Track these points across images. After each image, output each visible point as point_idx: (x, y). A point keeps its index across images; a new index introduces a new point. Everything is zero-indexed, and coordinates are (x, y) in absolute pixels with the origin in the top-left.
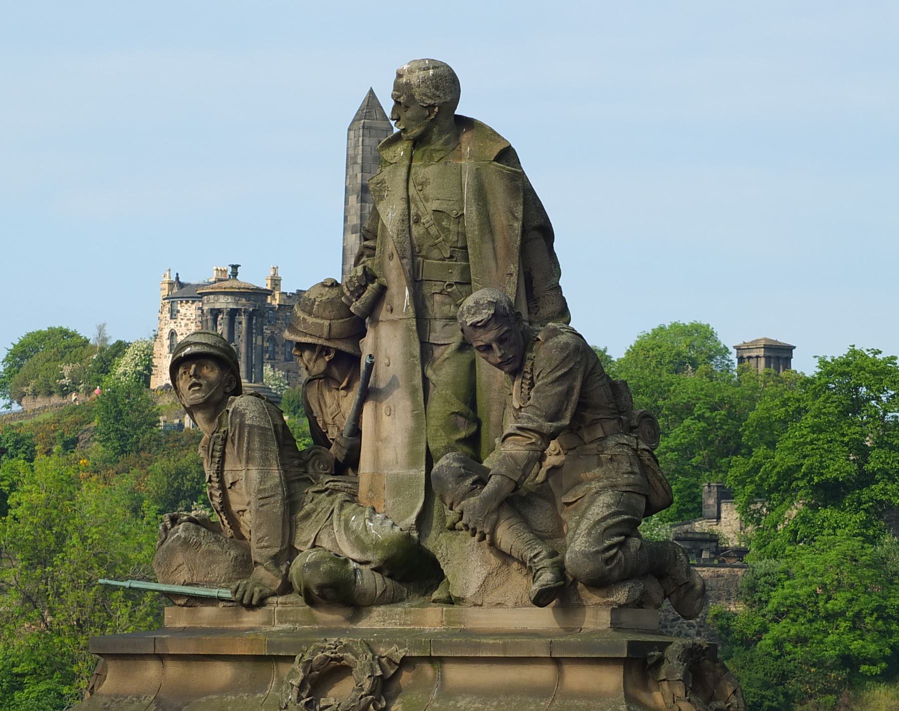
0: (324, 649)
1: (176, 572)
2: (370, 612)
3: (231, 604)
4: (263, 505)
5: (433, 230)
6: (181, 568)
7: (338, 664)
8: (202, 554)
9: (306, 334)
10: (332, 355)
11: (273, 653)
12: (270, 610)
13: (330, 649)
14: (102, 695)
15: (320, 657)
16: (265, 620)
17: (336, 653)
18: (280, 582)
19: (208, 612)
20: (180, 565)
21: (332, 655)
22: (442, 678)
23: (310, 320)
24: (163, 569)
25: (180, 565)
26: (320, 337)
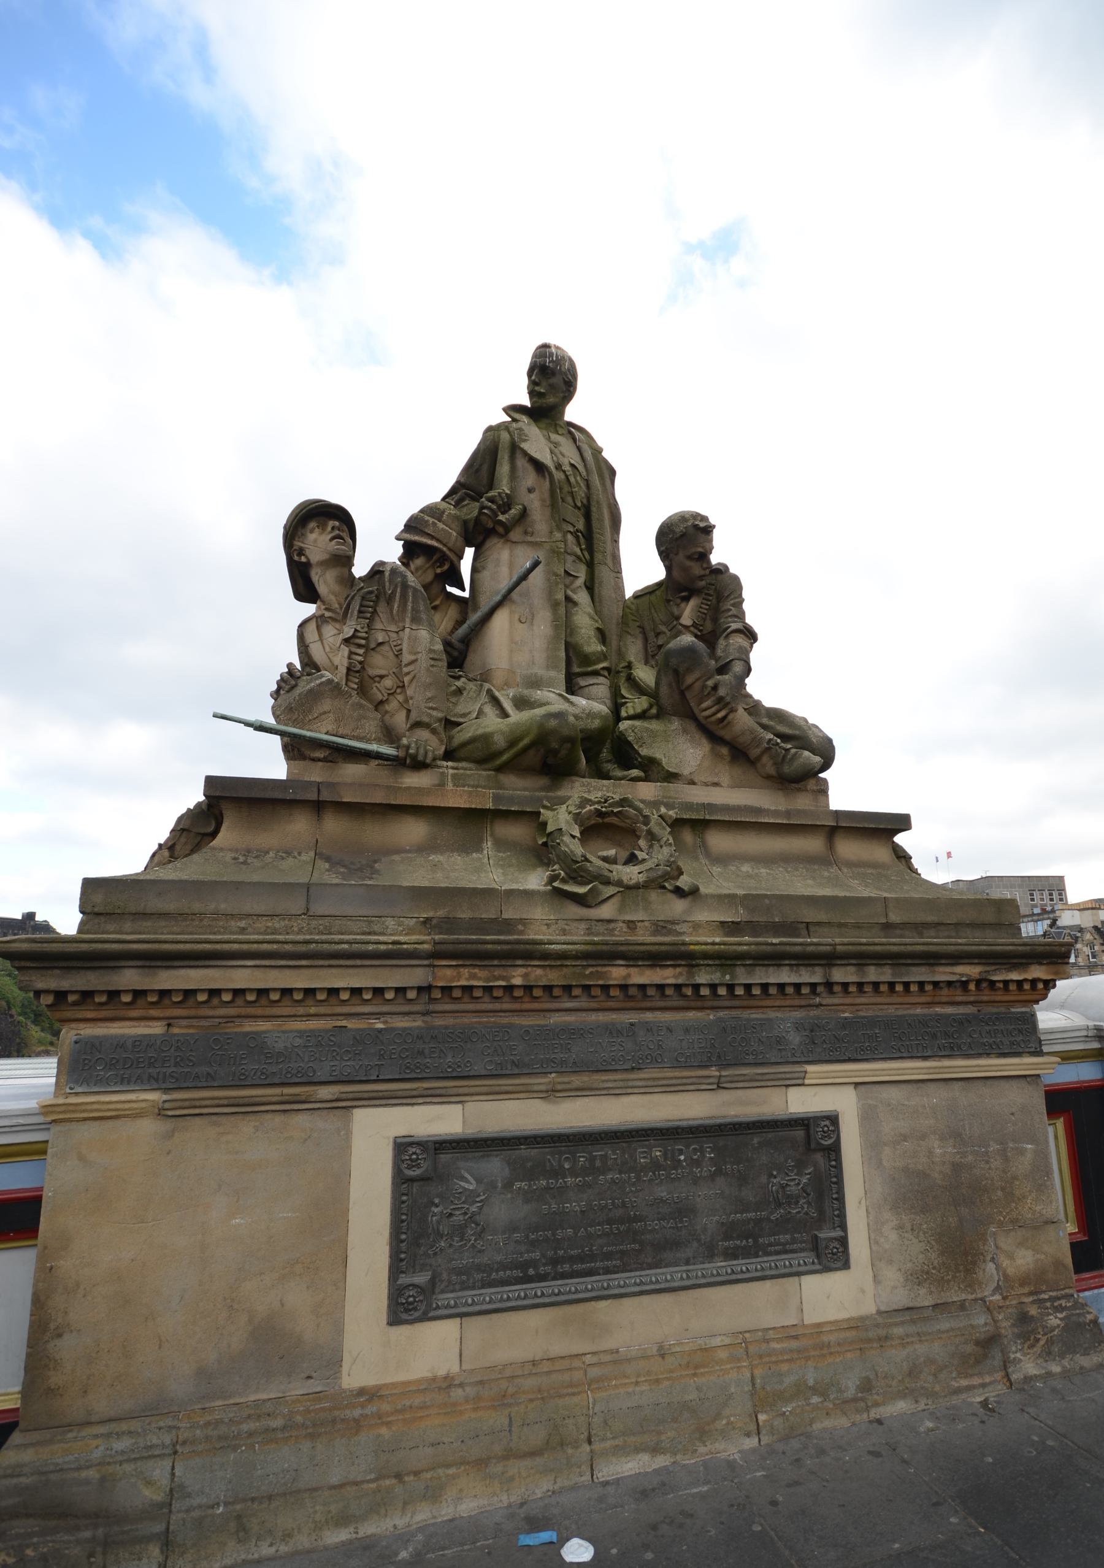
0: (592, 803)
1: (317, 721)
2: (573, 782)
3: (389, 763)
4: (432, 666)
5: (572, 479)
6: (323, 716)
7: (601, 821)
8: (352, 705)
9: (432, 537)
10: (446, 567)
11: (501, 807)
12: (443, 773)
13: (599, 802)
14: (222, 850)
15: (590, 810)
16: (436, 782)
17: (606, 807)
18: (443, 748)
19: (352, 771)
20: (325, 713)
21: (604, 809)
22: (704, 845)
23: (441, 525)
24: (296, 716)
25: (325, 713)
26: (445, 545)
